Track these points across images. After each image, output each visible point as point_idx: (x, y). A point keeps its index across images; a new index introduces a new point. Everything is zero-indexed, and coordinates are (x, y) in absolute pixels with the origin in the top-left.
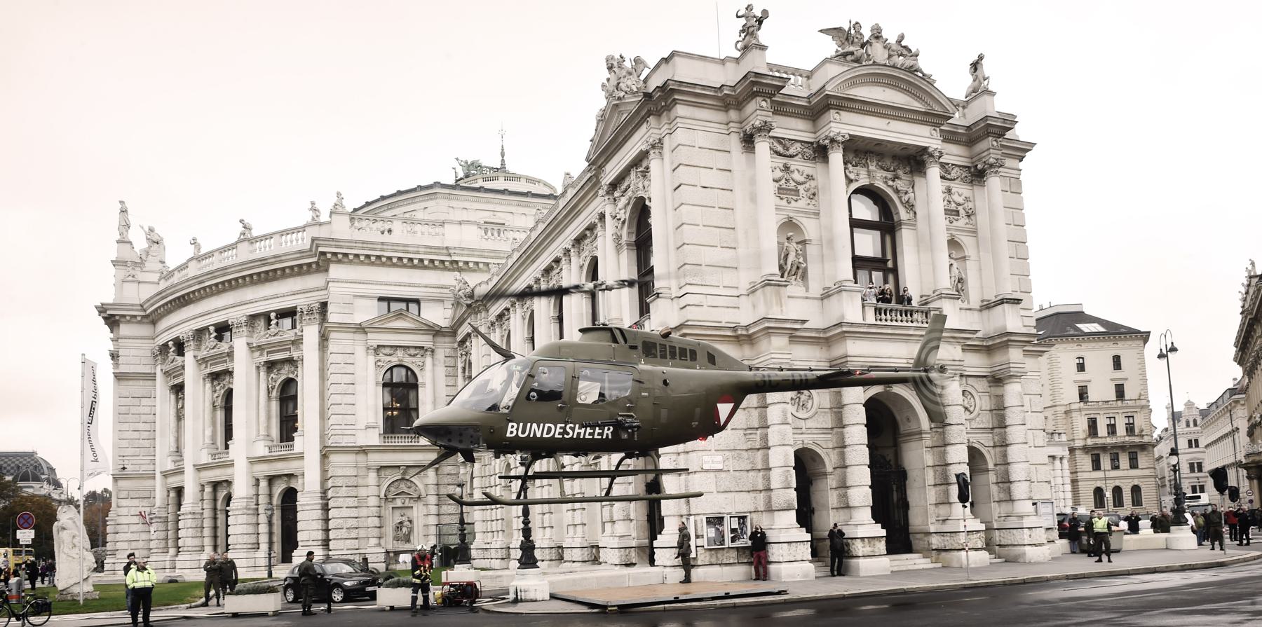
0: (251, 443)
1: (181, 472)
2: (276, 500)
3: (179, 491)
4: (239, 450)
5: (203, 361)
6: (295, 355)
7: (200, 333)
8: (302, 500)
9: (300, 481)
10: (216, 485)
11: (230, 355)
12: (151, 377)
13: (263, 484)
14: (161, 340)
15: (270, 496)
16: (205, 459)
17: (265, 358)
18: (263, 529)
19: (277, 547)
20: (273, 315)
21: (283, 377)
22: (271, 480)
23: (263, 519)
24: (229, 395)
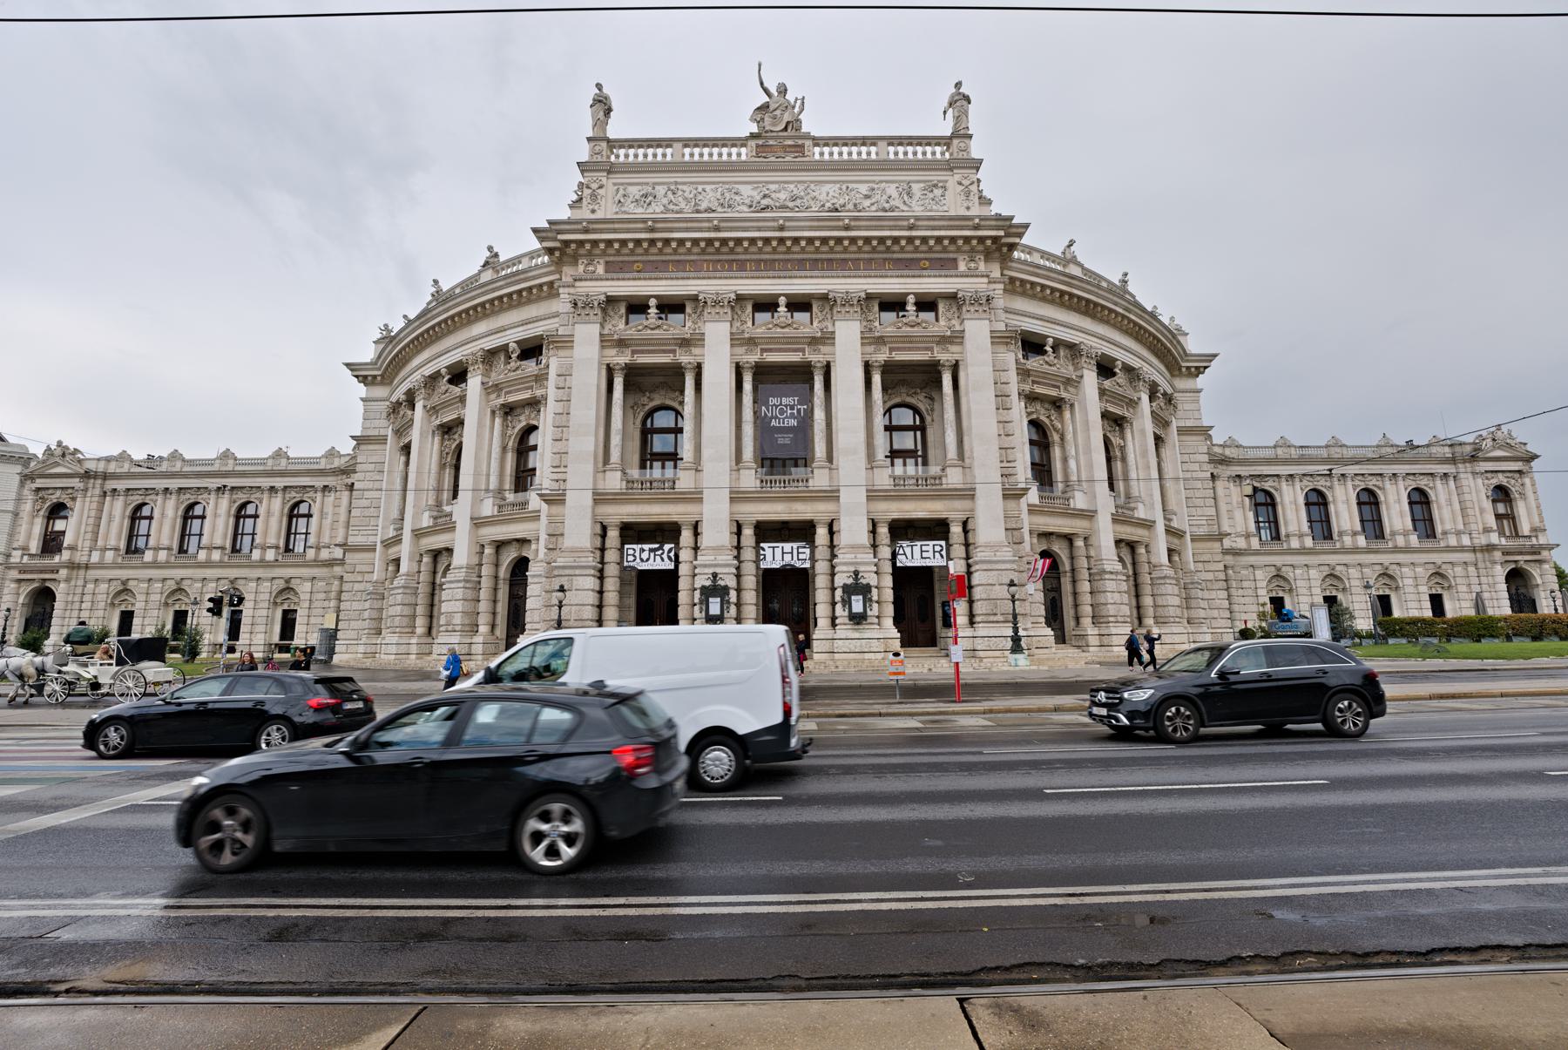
0: (477, 501)
1: (397, 540)
2: (504, 572)
3: (397, 562)
4: (461, 511)
5: (433, 411)
6: (539, 393)
7: (435, 377)
8: (534, 570)
9: (533, 546)
10: (436, 554)
11: (462, 399)
12: (382, 440)
13: (488, 551)
14: (394, 399)
15: (497, 565)
16: (426, 521)
17: (501, 401)
18: (484, 606)
19: (501, 631)
20: (513, 346)
21: (524, 424)
22: (500, 546)
23: (484, 594)
24: (459, 448)
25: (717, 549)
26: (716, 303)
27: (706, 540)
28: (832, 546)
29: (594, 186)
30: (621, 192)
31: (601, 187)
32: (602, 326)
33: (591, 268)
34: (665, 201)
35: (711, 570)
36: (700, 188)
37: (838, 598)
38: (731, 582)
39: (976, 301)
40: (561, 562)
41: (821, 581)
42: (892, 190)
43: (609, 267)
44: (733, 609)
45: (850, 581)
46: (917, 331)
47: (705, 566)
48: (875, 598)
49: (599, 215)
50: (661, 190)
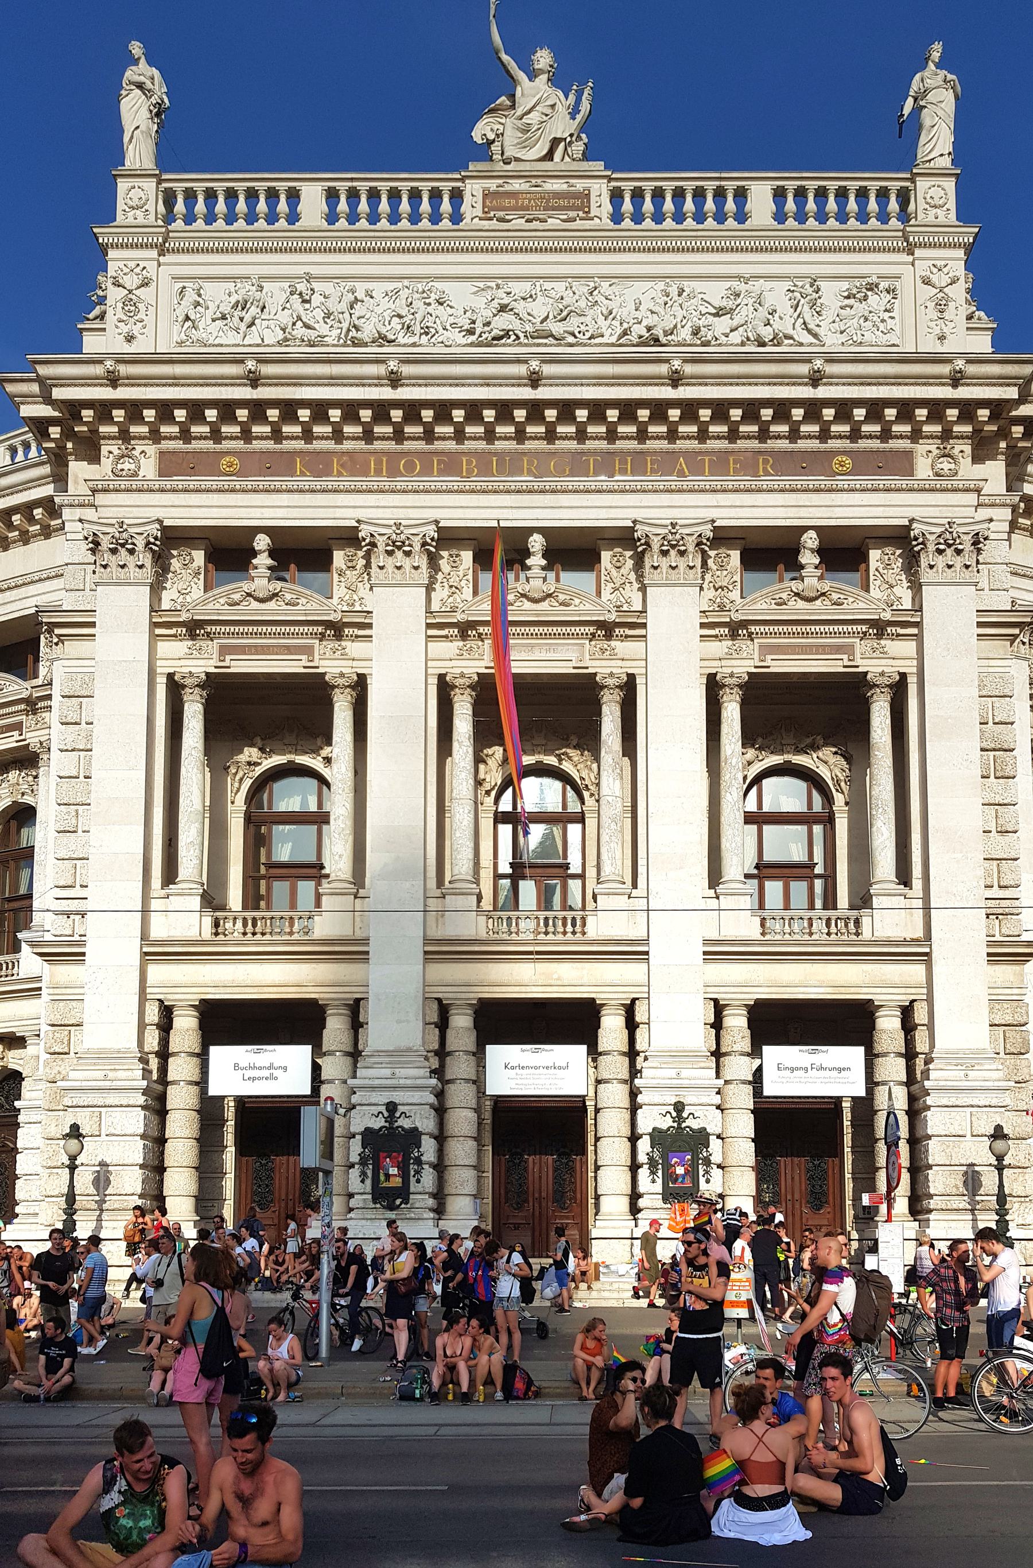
25: (397, 1055)
26: (396, 546)
27: (377, 1036)
28: (632, 1053)
29: (131, 281)
30: (191, 296)
31: (145, 284)
32: (157, 588)
33: (127, 465)
34: (285, 318)
35: (384, 1098)
36: (361, 288)
37: (642, 1158)
38: (426, 1123)
39: (949, 543)
40: (78, 1077)
41: (610, 1125)
42: (777, 295)
43: (170, 466)
44: (428, 1178)
45: (666, 1123)
46: (820, 609)
47: (373, 1088)
48: (716, 1158)
49: (142, 346)
50: (276, 293)
